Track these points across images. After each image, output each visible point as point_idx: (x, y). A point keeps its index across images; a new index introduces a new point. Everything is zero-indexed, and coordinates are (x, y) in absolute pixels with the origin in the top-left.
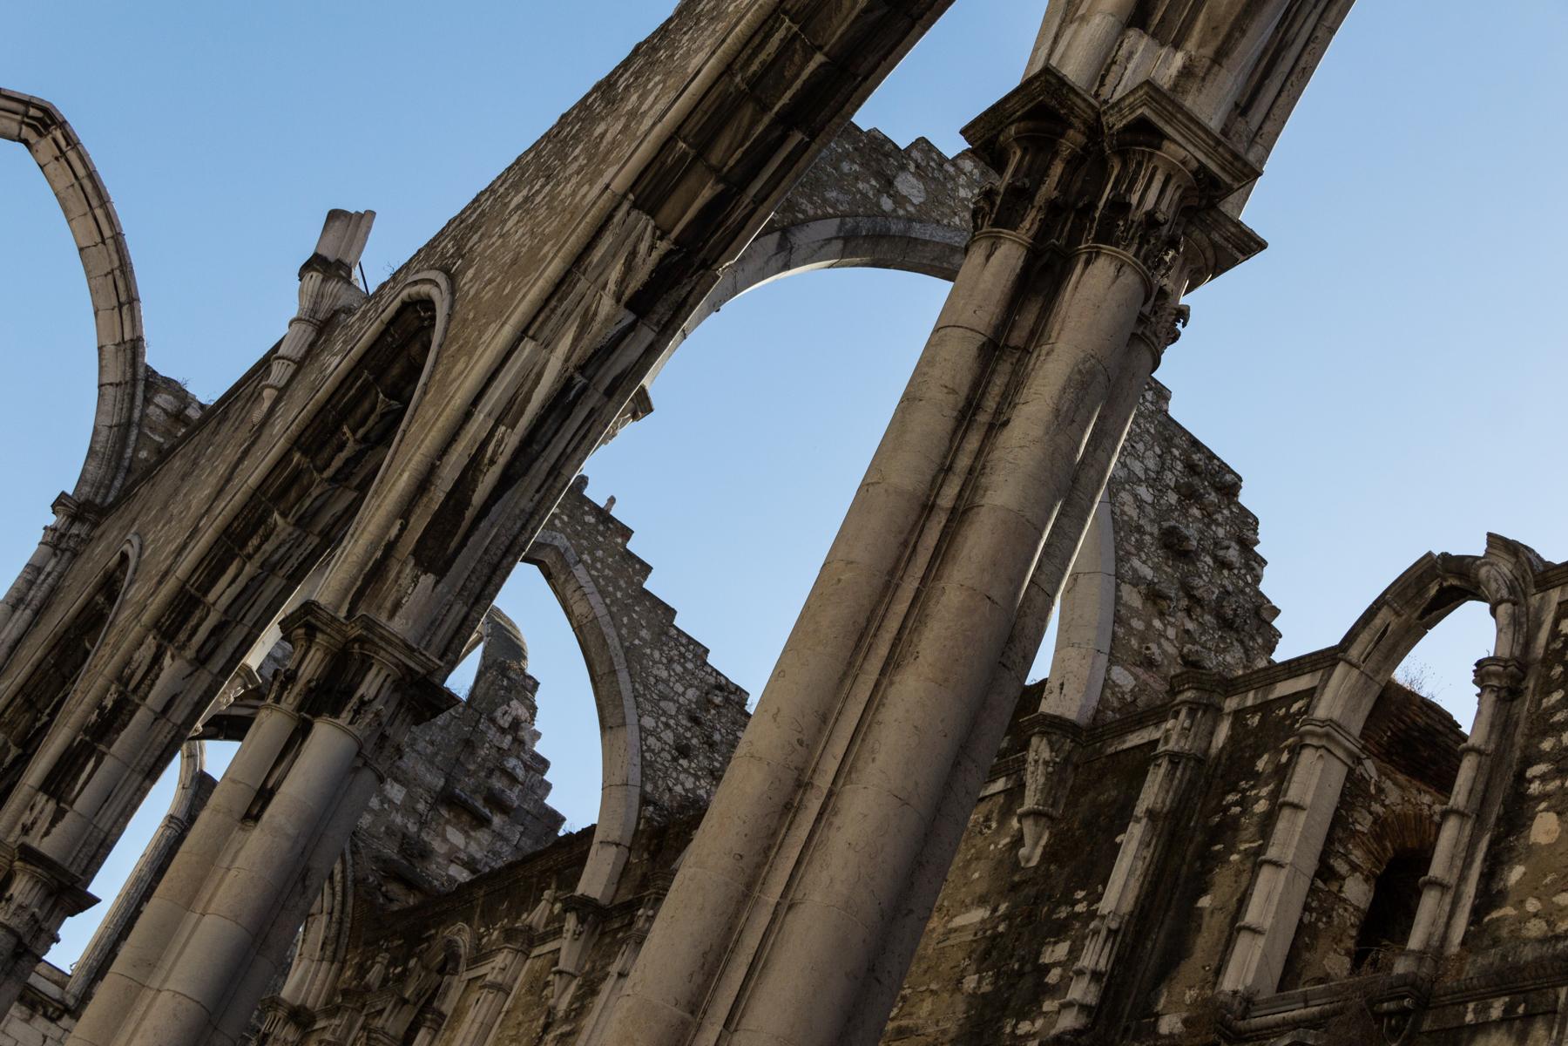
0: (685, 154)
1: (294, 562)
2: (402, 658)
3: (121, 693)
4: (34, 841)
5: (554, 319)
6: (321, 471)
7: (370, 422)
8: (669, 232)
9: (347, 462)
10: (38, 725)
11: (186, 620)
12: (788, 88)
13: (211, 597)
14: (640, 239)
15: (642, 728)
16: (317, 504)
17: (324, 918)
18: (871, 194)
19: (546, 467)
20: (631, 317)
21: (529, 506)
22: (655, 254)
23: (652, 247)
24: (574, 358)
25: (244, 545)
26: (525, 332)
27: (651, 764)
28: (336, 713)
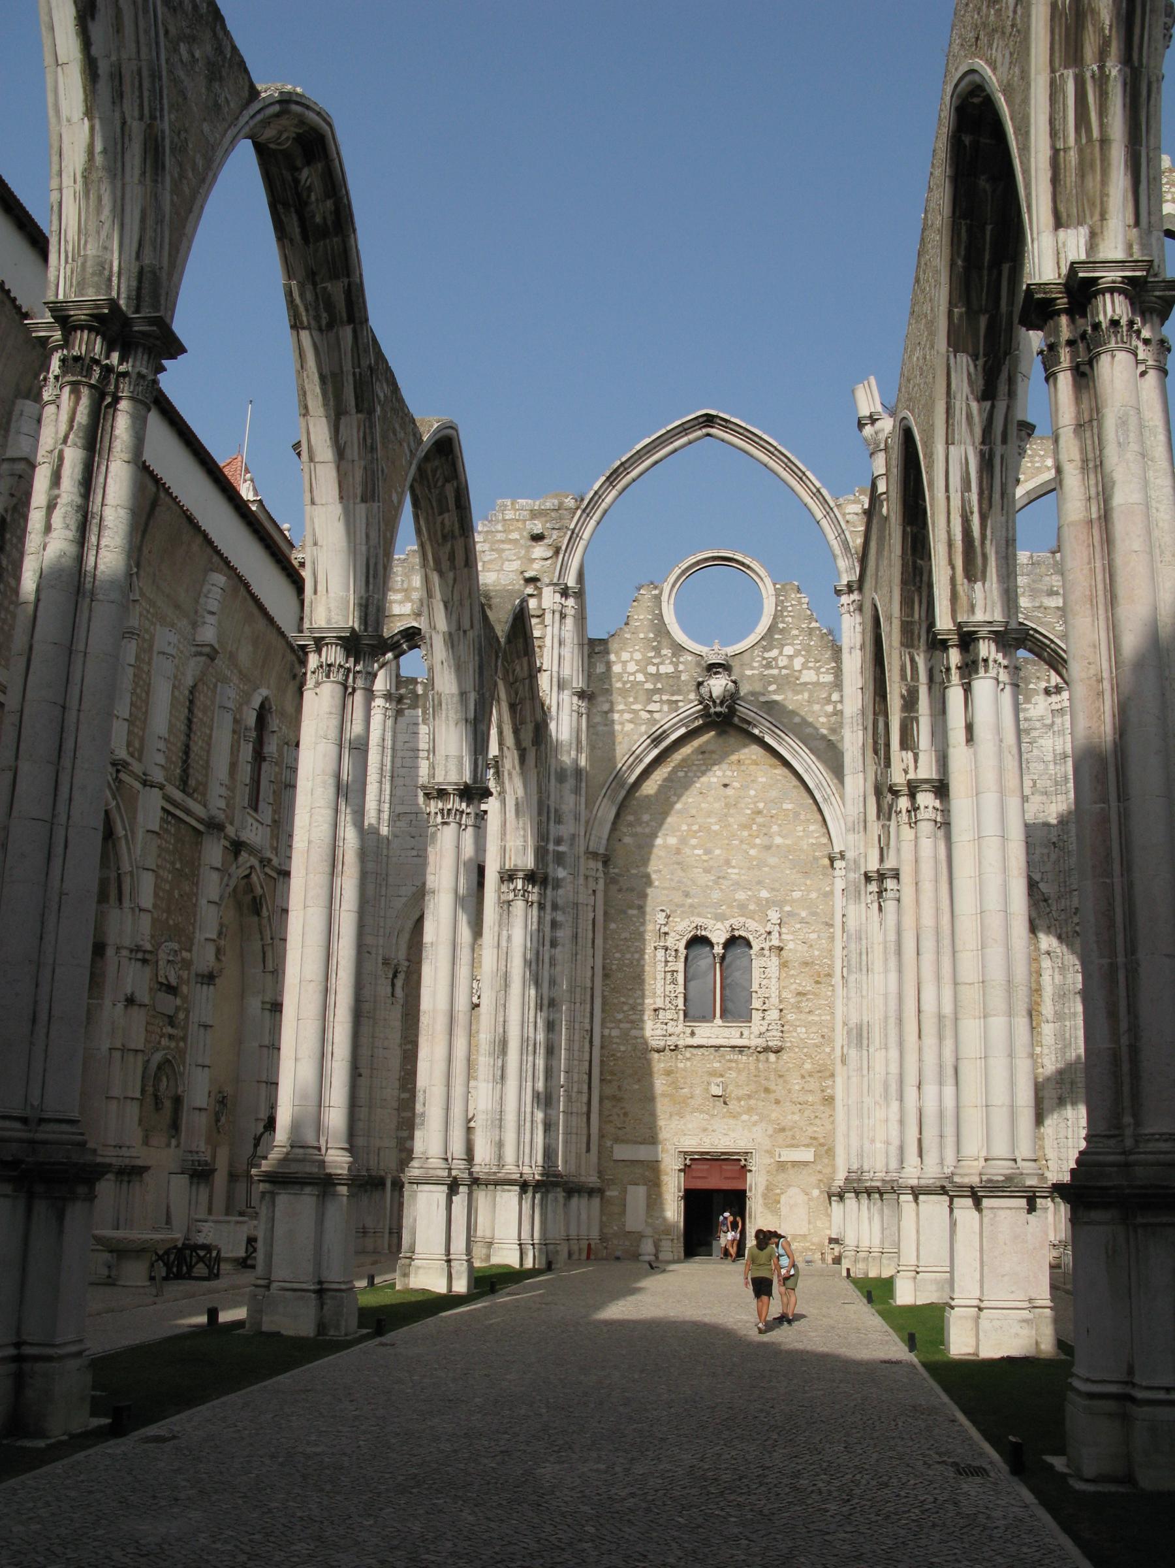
0: (961, 315)
4: (911, 776)
11: (912, 634)
12: (984, 250)
20: (988, 404)
21: (1004, 519)
22: (980, 368)
23: (976, 366)
26: (947, 443)
28: (977, 672)
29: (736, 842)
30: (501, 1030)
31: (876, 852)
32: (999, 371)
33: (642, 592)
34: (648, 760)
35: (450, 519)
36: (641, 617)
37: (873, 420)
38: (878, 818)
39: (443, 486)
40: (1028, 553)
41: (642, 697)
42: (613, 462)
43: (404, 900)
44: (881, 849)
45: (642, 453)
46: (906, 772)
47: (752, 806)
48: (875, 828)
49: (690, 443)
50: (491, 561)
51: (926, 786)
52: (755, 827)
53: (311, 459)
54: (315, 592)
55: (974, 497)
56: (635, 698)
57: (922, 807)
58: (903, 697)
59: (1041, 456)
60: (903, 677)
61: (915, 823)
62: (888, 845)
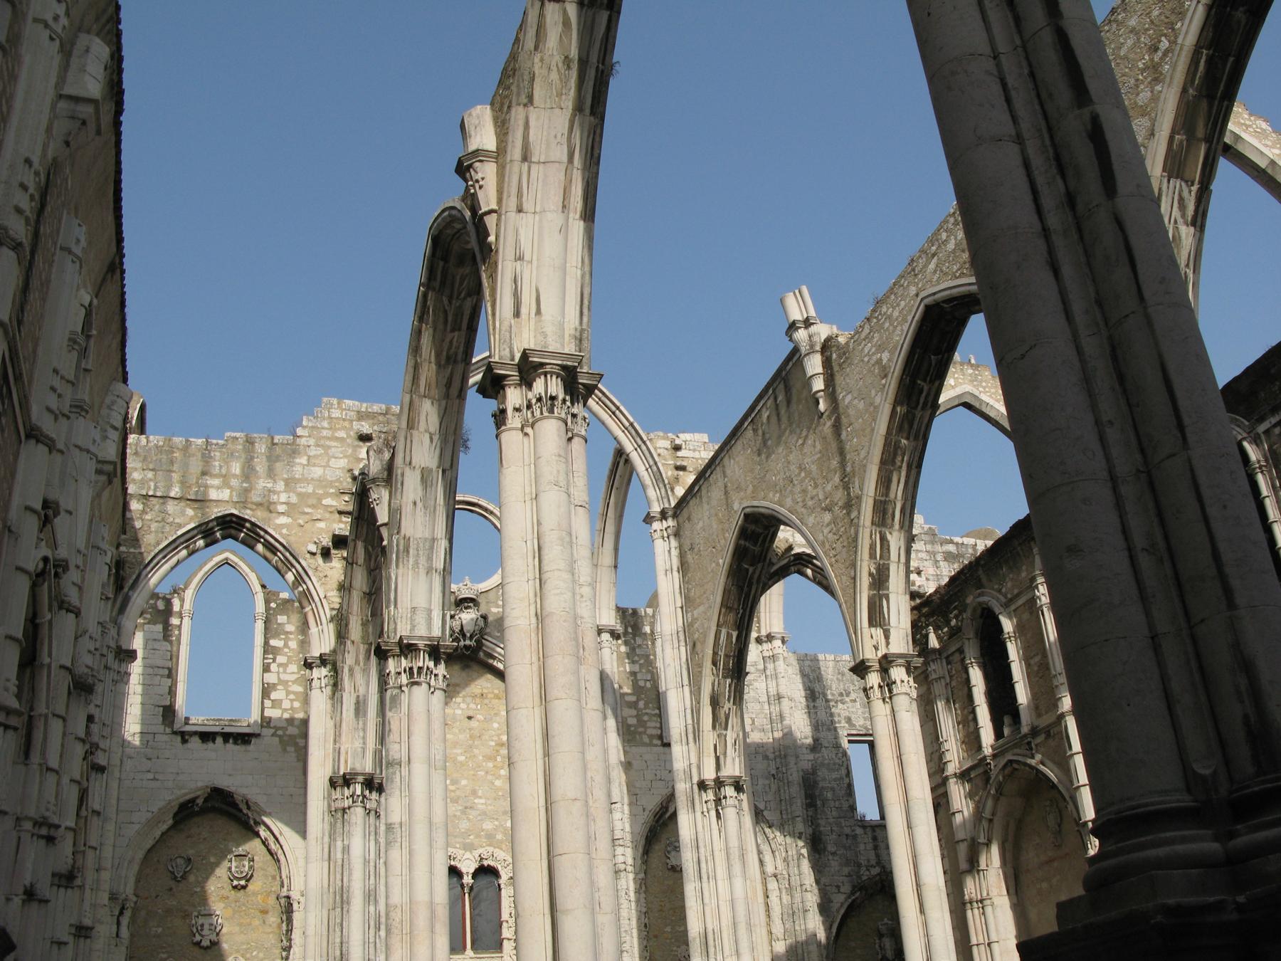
13: (892, 495)
14: (1181, 190)
29: (482, 773)
30: (338, 953)
35: (458, 337)
37: (807, 323)
38: (714, 727)
39: (465, 298)
43: (137, 827)
44: (717, 759)
46: (876, 648)
48: (709, 737)
50: (316, 457)
51: (901, 661)
52: (499, 759)
53: (525, 158)
54: (517, 314)
57: (898, 682)
58: (871, 574)
60: (872, 555)
61: (890, 698)
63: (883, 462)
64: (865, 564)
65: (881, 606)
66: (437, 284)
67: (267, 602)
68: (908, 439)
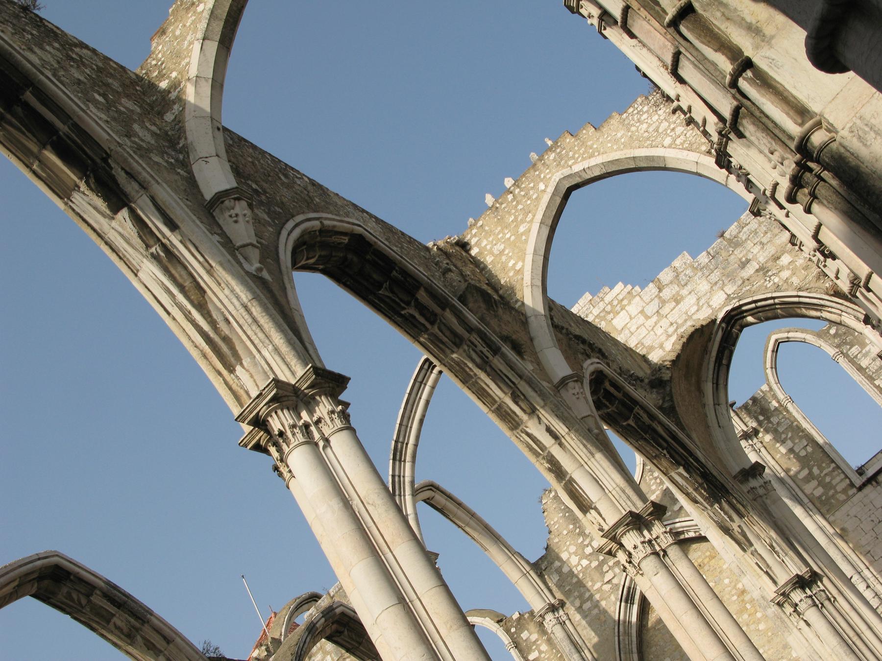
1: (485, 350)
2: (264, 402)
3: (544, 458)
4: (606, 528)
5: (128, 256)
6: (427, 329)
7: (397, 300)
8: (75, 182)
9: (422, 314)
10: (668, 456)
11: (509, 414)
13: (497, 398)
15: (670, 147)
16: (448, 333)
17: (843, 314)
18: (193, 18)
19: (206, 277)
20: (124, 213)
23: (84, 194)
24: (142, 250)
25: (472, 377)
26: (136, 275)
27: (691, 144)
31: (766, 578)
32: (113, 179)
33: (544, 502)
34: (634, 619)
35: (120, 619)
36: (556, 519)
38: (744, 550)
39: (89, 601)
40: (704, 253)
41: (596, 576)
42: (390, 444)
44: (767, 573)
45: (405, 423)
47: (734, 592)
49: (433, 388)
51: (620, 531)
52: (748, 606)
55: (180, 298)
56: (592, 580)
58: (550, 470)
59: (532, 188)
60: (537, 455)
62: (768, 566)
63: (464, 382)
64: (537, 465)
65: (576, 489)
66: (68, 609)
67: (508, 631)
68: (453, 352)
